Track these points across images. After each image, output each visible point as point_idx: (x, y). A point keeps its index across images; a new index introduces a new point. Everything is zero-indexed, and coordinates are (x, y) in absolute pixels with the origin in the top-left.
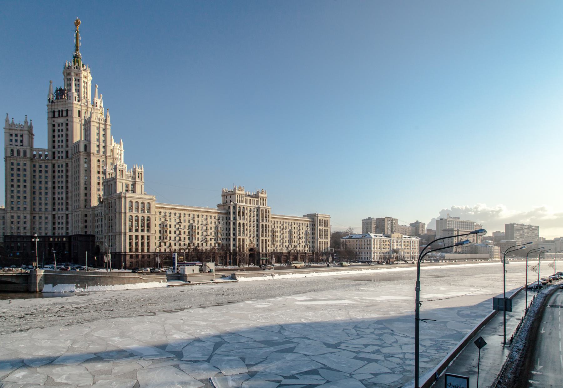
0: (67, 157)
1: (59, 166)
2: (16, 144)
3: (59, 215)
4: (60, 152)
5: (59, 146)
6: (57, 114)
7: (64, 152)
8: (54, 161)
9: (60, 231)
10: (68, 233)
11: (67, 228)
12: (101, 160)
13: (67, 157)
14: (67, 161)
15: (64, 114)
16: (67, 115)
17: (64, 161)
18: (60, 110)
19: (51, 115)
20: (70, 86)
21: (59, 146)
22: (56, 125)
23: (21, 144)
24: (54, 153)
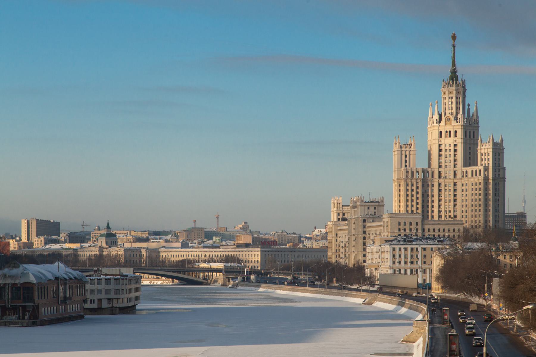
1: (446, 186)
12: (497, 182)
16: (456, 136)
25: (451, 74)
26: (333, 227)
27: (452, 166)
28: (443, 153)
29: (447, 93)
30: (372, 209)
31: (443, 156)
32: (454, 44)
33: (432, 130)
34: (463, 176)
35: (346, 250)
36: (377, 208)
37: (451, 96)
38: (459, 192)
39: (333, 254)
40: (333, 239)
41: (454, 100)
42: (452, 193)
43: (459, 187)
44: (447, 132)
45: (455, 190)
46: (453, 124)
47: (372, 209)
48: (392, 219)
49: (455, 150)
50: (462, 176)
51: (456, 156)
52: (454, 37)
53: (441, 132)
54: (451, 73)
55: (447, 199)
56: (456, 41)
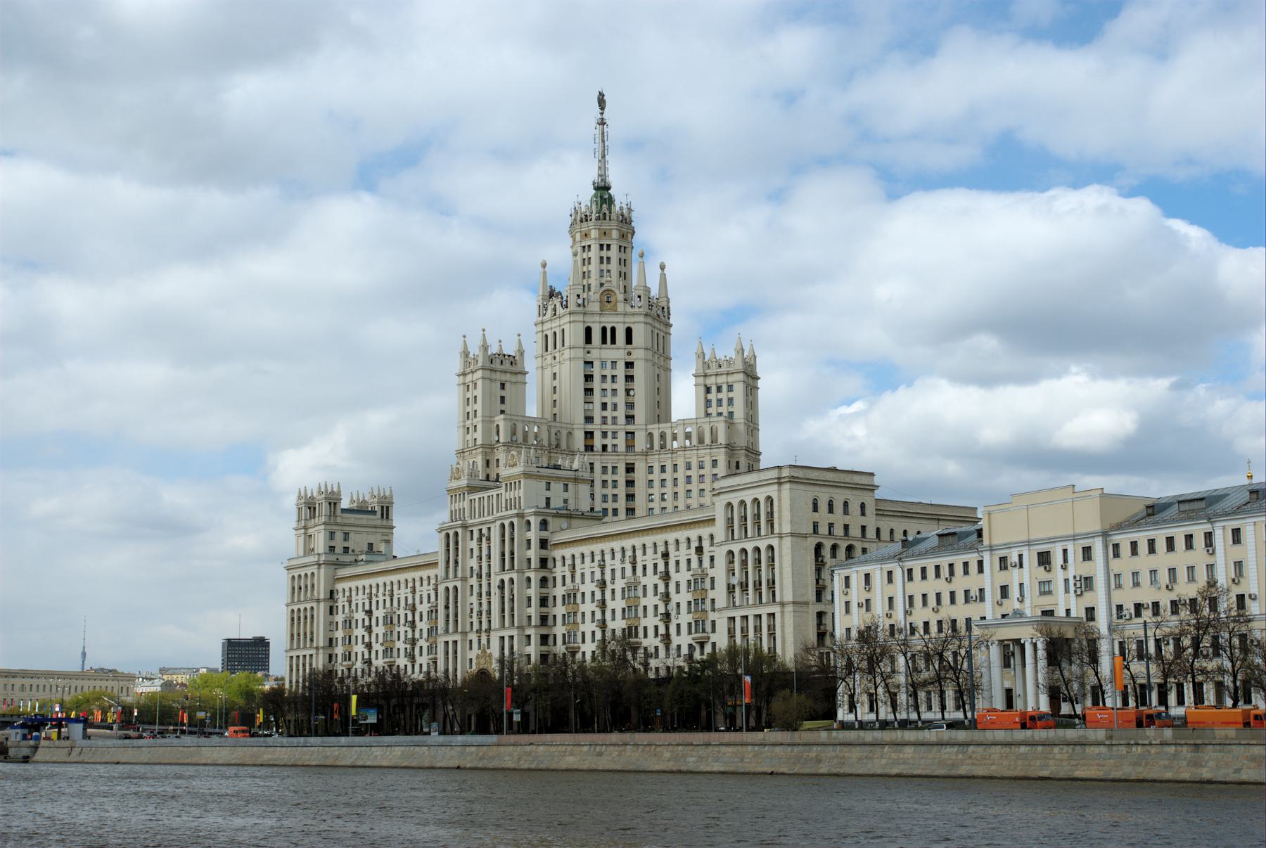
0: (630, 447)
1: (605, 469)
4: (610, 434)
5: (605, 418)
13: (630, 447)
16: (629, 340)
17: (623, 457)
21: (605, 418)
22: (597, 364)
24: (589, 435)
25: (594, 191)
26: (322, 571)
28: (597, 384)
29: (594, 234)
30: (557, 487)
31: (597, 392)
32: (602, 119)
33: (564, 324)
34: (652, 447)
35: (395, 634)
36: (571, 486)
37: (605, 242)
38: (640, 489)
39: (321, 651)
40: (318, 608)
41: (614, 253)
42: (622, 491)
43: (640, 475)
44: (604, 330)
45: (630, 483)
46: (621, 307)
47: (557, 487)
48: (795, 486)
49: (629, 378)
50: (648, 446)
51: (632, 393)
52: (602, 102)
53: (588, 331)
54: (595, 189)
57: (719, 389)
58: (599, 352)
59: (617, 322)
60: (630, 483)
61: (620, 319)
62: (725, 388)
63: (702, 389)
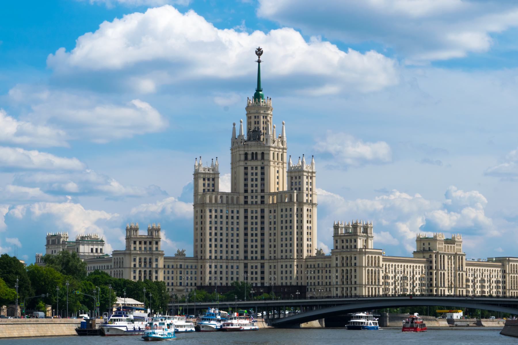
0: (262, 202)
1: (252, 212)
2: (208, 188)
3: (252, 265)
4: (254, 197)
6: (250, 157)
7: (259, 197)
8: (246, 207)
9: (254, 281)
10: (262, 284)
11: (262, 278)
12: (309, 209)
13: (262, 202)
14: (262, 207)
15: (259, 157)
16: (263, 158)
17: (259, 206)
18: (254, 153)
19: (243, 157)
20: (258, 124)
22: (249, 168)
23: (213, 188)
24: (246, 197)
27: (259, 191)
32: (259, 60)
37: (257, 115)
53: (246, 154)
55: (254, 226)
56: (262, 57)
57: (296, 178)
58: (250, 163)
59: (258, 150)
60: (263, 217)
61: (259, 149)
62: (298, 178)
63: (290, 178)
